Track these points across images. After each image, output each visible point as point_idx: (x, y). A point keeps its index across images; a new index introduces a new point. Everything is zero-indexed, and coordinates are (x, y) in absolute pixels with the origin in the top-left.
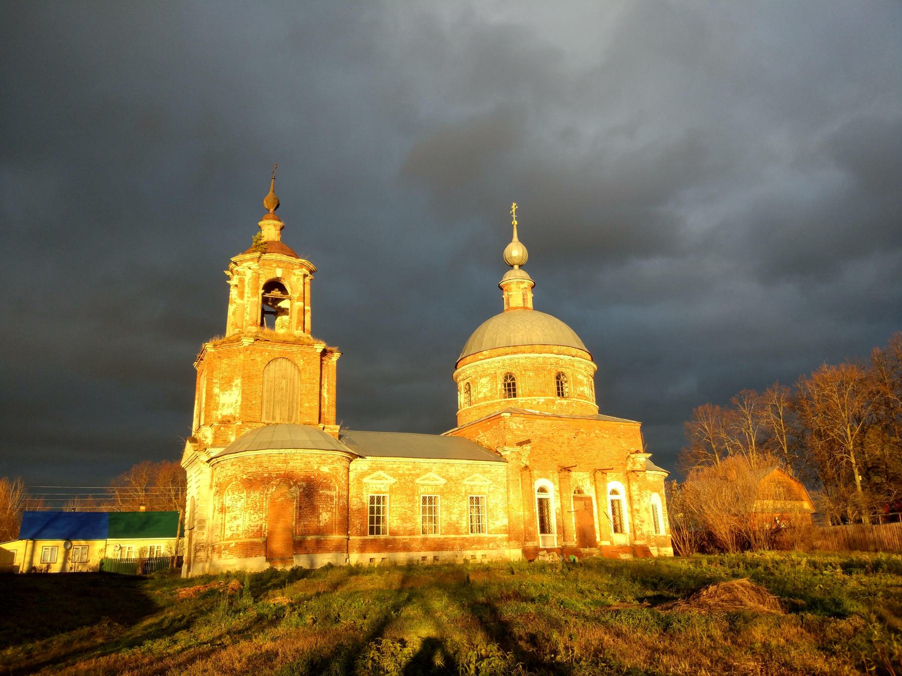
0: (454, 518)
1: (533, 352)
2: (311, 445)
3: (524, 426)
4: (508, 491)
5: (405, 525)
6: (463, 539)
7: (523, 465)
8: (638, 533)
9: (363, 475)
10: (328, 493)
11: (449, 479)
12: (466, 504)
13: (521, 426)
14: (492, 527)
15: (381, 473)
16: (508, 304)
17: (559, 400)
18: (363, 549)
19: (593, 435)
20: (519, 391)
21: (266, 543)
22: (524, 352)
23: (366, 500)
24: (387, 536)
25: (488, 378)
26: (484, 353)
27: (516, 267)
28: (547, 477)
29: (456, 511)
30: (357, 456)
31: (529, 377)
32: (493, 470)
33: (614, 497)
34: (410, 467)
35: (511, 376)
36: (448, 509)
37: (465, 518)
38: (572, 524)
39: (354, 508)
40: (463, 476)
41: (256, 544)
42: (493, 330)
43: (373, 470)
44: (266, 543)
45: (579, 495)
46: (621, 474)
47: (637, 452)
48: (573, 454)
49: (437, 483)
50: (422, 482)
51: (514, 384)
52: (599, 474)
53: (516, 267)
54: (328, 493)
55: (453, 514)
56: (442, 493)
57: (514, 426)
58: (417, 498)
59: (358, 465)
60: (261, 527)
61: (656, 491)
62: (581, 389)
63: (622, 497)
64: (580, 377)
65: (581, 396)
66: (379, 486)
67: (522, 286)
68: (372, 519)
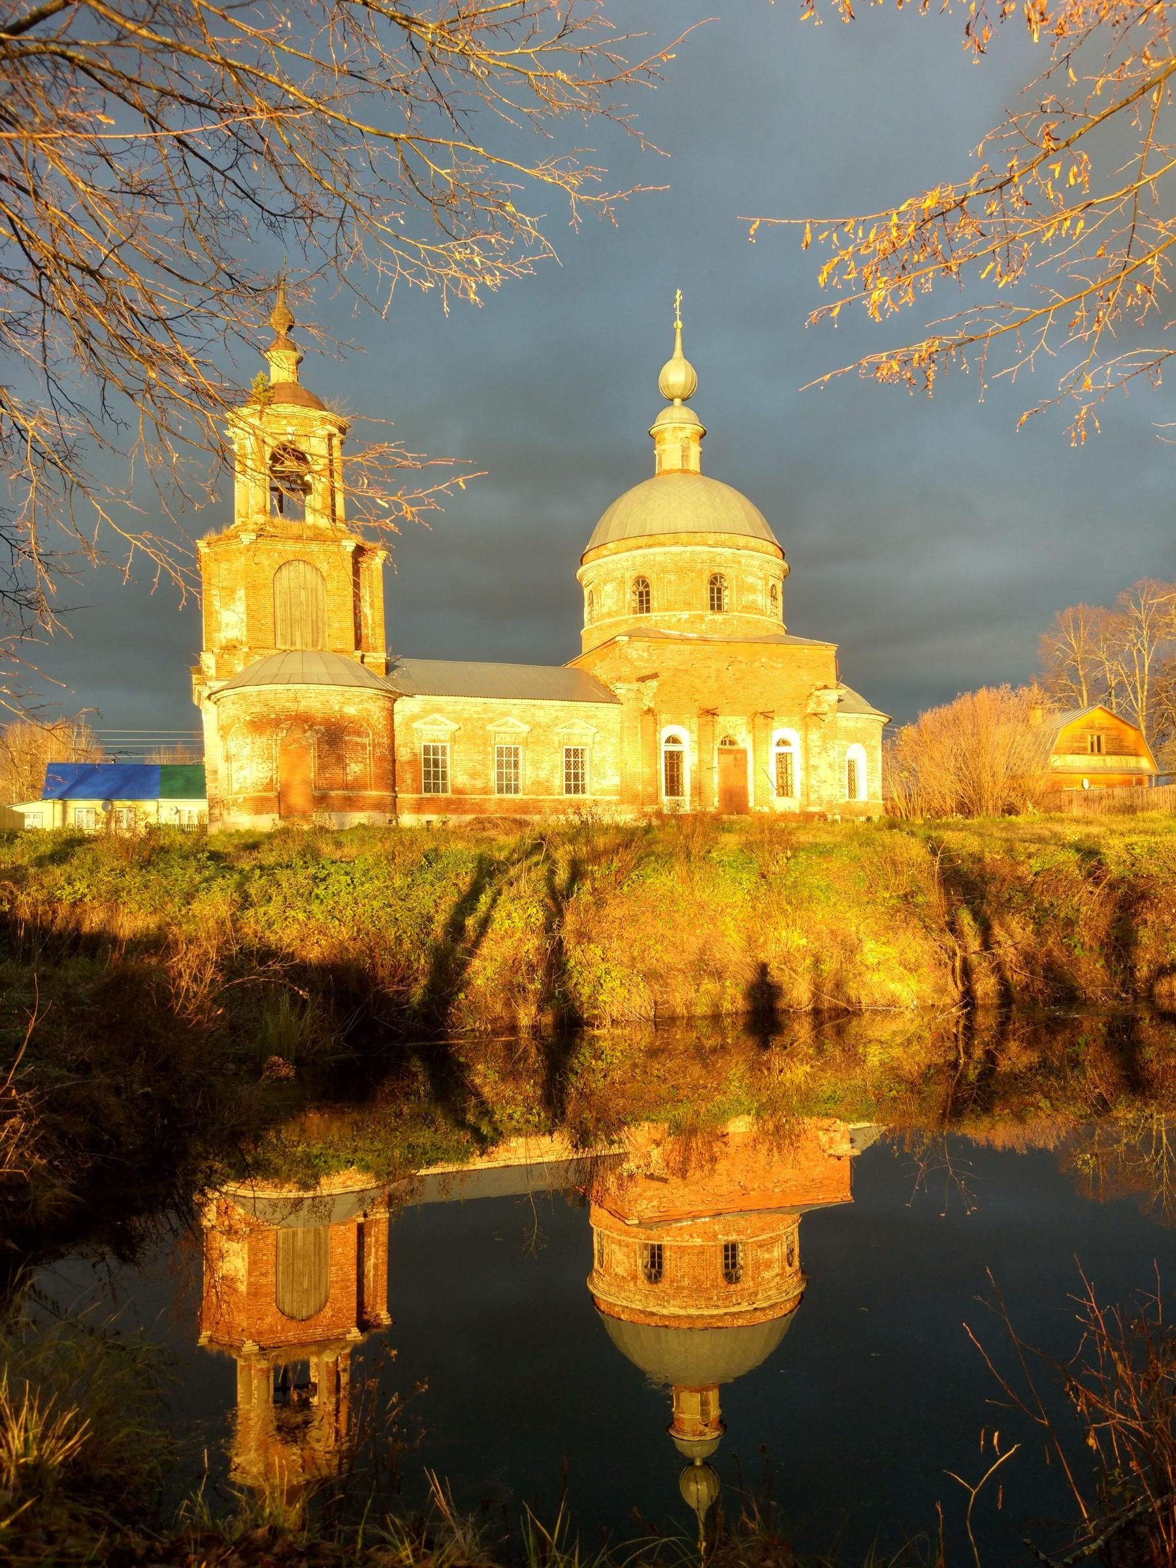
0: (543, 775)
1: (677, 543)
2: (327, 679)
3: (650, 655)
4: (622, 741)
5: (473, 782)
6: (554, 801)
7: (645, 708)
8: (813, 797)
9: (414, 718)
10: (359, 740)
11: (535, 726)
12: (560, 758)
13: (645, 655)
14: (596, 786)
15: (437, 716)
16: (660, 463)
17: (710, 616)
18: (419, 807)
19: (756, 665)
20: (654, 604)
21: (281, 797)
22: (663, 545)
23: (419, 749)
24: (449, 795)
25: (614, 584)
26: (610, 545)
27: (677, 401)
28: (682, 724)
29: (546, 766)
30: (401, 695)
31: (669, 582)
32: (600, 714)
33: (782, 749)
34: (479, 709)
35: (644, 582)
36: (536, 764)
37: (558, 775)
38: (714, 783)
39: (404, 759)
40: (555, 721)
41: (267, 799)
42: (636, 508)
43: (427, 712)
44: (281, 797)
45: (728, 747)
46: (797, 719)
47: (825, 687)
48: (723, 692)
49: (517, 730)
50: (497, 729)
51: (648, 594)
52: (760, 720)
53: (677, 401)
54: (359, 740)
55: (541, 772)
56: (526, 744)
57: (633, 654)
58: (489, 749)
59: (404, 707)
60: (271, 780)
61: (858, 741)
62: (751, 597)
63: (795, 750)
64: (750, 580)
65: (751, 608)
66: (435, 733)
67: (682, 435)
68: (427, 773)
